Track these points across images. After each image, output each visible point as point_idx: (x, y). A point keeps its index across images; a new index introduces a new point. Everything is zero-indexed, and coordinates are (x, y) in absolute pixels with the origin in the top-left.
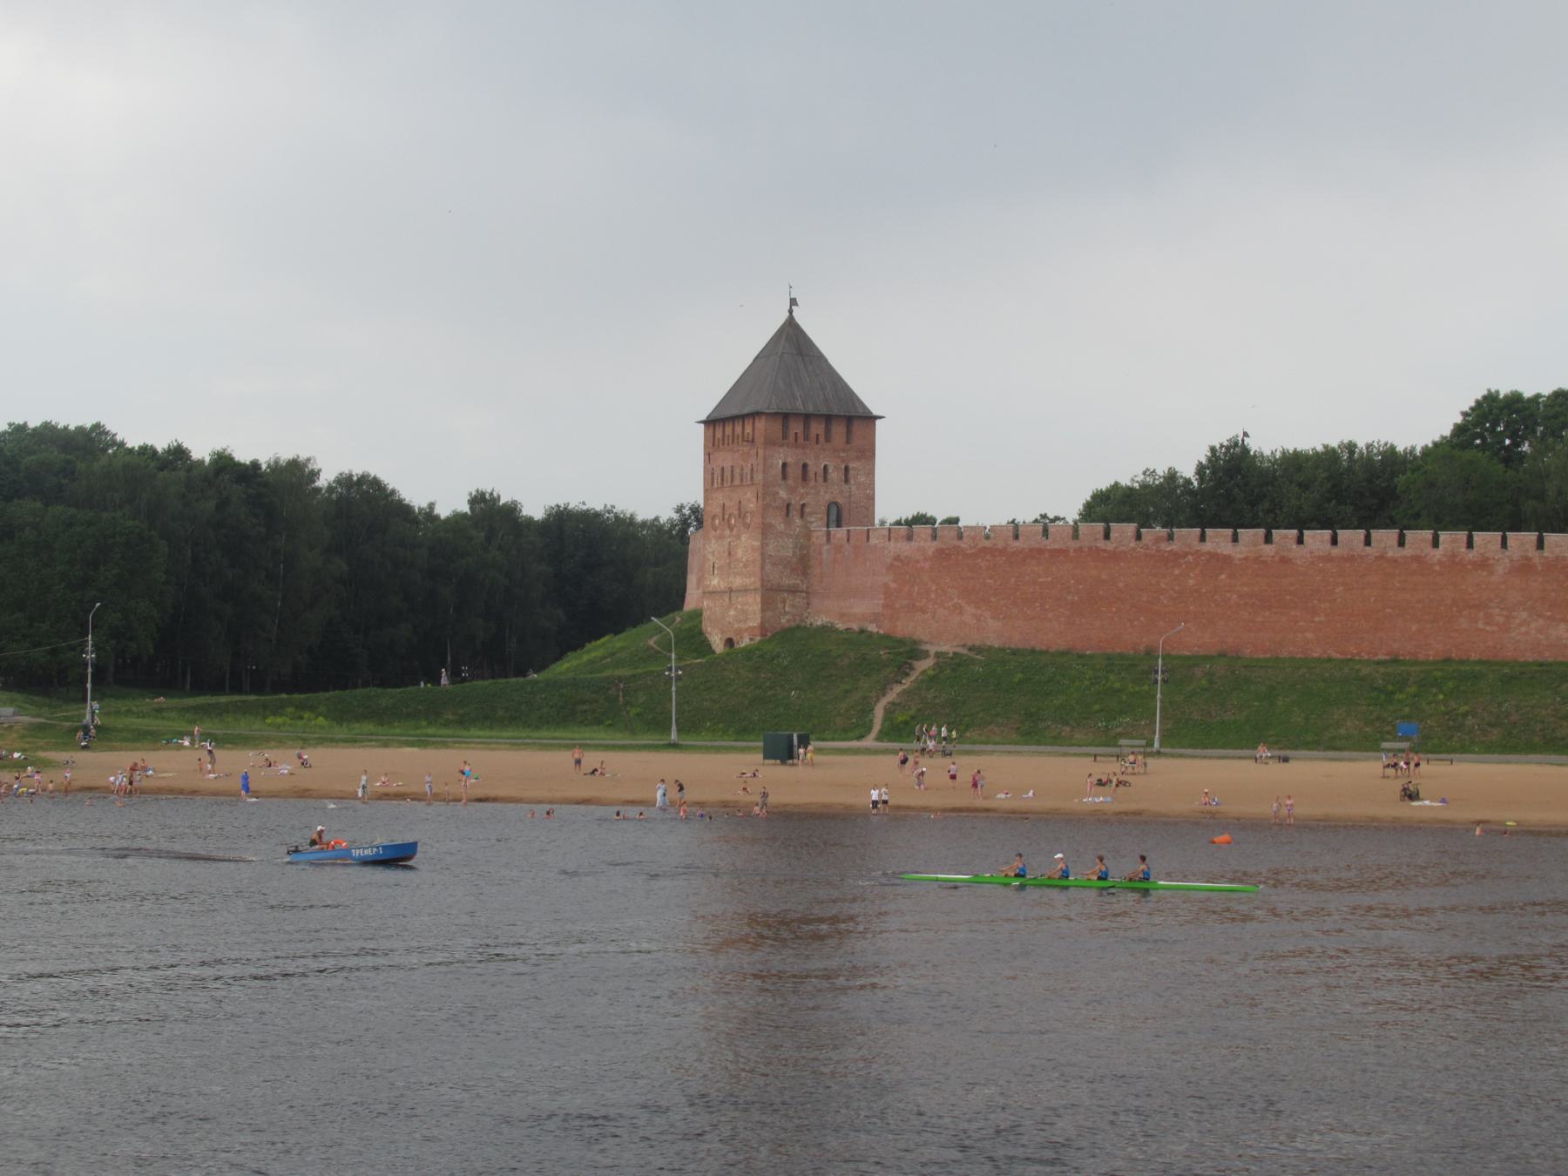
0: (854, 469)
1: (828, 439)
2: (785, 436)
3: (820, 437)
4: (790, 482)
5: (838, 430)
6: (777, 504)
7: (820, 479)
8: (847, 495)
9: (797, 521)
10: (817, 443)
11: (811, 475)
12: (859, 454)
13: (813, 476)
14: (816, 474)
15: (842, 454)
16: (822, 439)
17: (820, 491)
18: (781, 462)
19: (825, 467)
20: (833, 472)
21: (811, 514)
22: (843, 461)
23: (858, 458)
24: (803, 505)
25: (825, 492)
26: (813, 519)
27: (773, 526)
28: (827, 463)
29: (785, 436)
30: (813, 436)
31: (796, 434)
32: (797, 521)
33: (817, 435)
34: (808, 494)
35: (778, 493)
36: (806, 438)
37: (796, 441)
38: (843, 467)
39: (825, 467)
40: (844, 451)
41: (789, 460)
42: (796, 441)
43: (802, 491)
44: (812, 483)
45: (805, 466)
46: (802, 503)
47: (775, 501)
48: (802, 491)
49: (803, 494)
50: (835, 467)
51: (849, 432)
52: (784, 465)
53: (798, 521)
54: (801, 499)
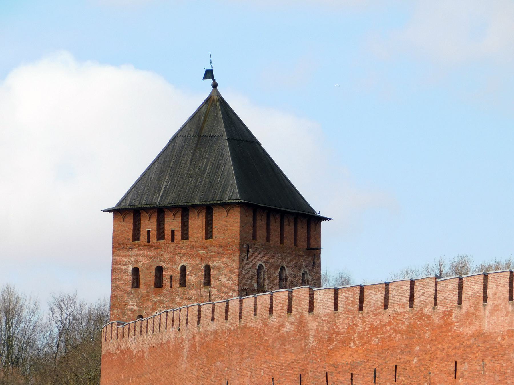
0: (216, 268)
1: (185, 236)
2: (136, 237)
3: (176, 233)
4: (142, 290)
7: (176, 283)
10: (173, 240)
11: (166, 279)
12: (221, 250)
16: (178, 235)
18: (131, 267)
19: (184, 269)
23: (220, 255)
28: (185, 264)
31: (149, 232)
36: (160, 236)
38: (202, 266)
39: (184, 269)
40: (203, 247)
41: (140, 264)
44: (166, 288)
45: (160, 270)
49: (155, 303)
51: (209, 224)
52: (136, 271)
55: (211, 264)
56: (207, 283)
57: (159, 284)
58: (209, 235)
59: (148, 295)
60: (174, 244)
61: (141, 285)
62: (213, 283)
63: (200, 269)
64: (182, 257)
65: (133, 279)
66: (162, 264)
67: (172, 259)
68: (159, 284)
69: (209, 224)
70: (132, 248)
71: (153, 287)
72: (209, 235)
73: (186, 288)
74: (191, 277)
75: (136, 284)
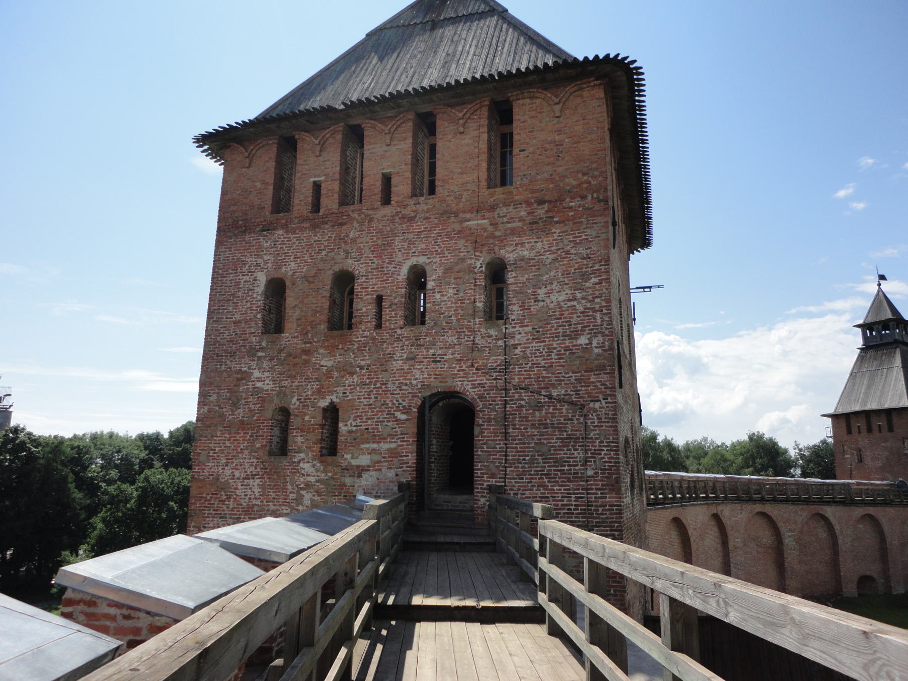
0: (523, 264)
4: (289, 337)
6: (240, 413)
7: (394, 316)
8: (496, 360)
9: (306, 467)
10: (386, 200)
11: (364, 307)
13: (371, 309)
14: (380, 299)
15: (475, 222)
16: (402, 187)
17: (391, 356)
18: (262, 278)
20: (440, 282)
21: (356, 440)
22: (477, 245)
26: (364, 460)
27: (225, 487)
28: (422, 260)
30: (372, 182)
31: (317, 186)
32: (306, 467)
33: (387, 180)
34: (347, 370)
35: (244, 376)
38: (480, 262)
41: (289, 269)
43: (327, 363)
44: (364, 331)
46: (324, 403)
47: (235, 405)
48: (327, 363)
49: (329, 374)
50: (448, 270)
54: (320, 393)
55: (509, 255)
59: (306, 352)
60: (388, 211)
61: (291, 326)
62: (514, 310)
63: (471, 270)
64: (411, 243)
65: (267, 310)
66: (350, 264)
67: (383, 248)
70: (268, 228)
71: (323, 327)
73: (424, 329)
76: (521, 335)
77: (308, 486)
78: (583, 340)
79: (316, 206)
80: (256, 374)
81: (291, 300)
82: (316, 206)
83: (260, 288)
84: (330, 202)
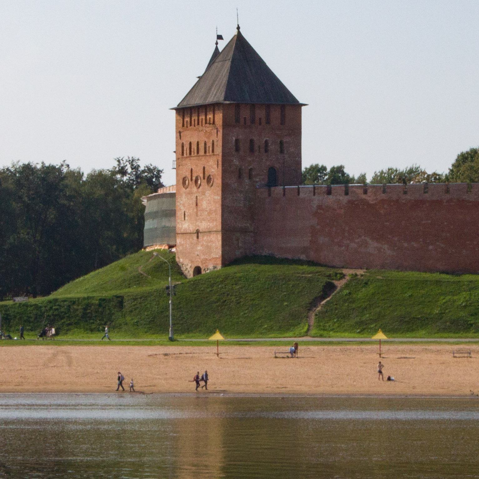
1: (268, 122)
2: (237, 121)
4: (241, 153)
5: (276, 114)
7: (263, 150)
10: (260, 124)
11: (256, 148)
16: (264, 120)
18: (234, 139)
24: (251, 170)
25: (266, 160)
26: (258, 180)
28: (268, 139)
29: (237, 121)
33: (260, 119)
35: (233, 161)
36: (253, 121)
37: (245, 124)
41: (240, 137)
42: (245, 124)
43: (250, 159)
44: (256, 153)
45: (252, 141)
46: (249, 168)
51: (283, 117)
52: (237, 141)
53: (247, 181)
55: (285, 140)
56: (282, 151)
57: (252, 150)
58: (283, 122)
62: (286, 152)
68: (252, 150)
69: (283, 117)
72: (283, 122)
74: (272, 147)
75: (237, 149)
76: (286, 156)
77: (247, 185)
78: (297, 159)
79: (245, 123)
80: (235, 160)
81: (241, 144)
82: (245, 123)
83: (234, 141)
84: (248, 123)
